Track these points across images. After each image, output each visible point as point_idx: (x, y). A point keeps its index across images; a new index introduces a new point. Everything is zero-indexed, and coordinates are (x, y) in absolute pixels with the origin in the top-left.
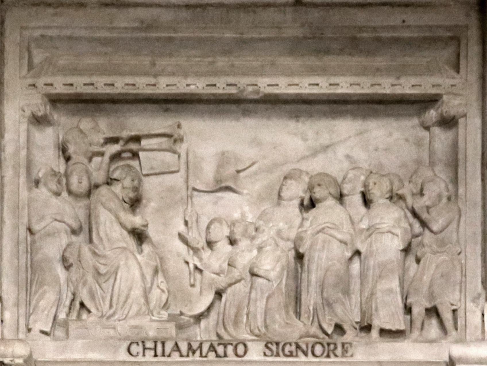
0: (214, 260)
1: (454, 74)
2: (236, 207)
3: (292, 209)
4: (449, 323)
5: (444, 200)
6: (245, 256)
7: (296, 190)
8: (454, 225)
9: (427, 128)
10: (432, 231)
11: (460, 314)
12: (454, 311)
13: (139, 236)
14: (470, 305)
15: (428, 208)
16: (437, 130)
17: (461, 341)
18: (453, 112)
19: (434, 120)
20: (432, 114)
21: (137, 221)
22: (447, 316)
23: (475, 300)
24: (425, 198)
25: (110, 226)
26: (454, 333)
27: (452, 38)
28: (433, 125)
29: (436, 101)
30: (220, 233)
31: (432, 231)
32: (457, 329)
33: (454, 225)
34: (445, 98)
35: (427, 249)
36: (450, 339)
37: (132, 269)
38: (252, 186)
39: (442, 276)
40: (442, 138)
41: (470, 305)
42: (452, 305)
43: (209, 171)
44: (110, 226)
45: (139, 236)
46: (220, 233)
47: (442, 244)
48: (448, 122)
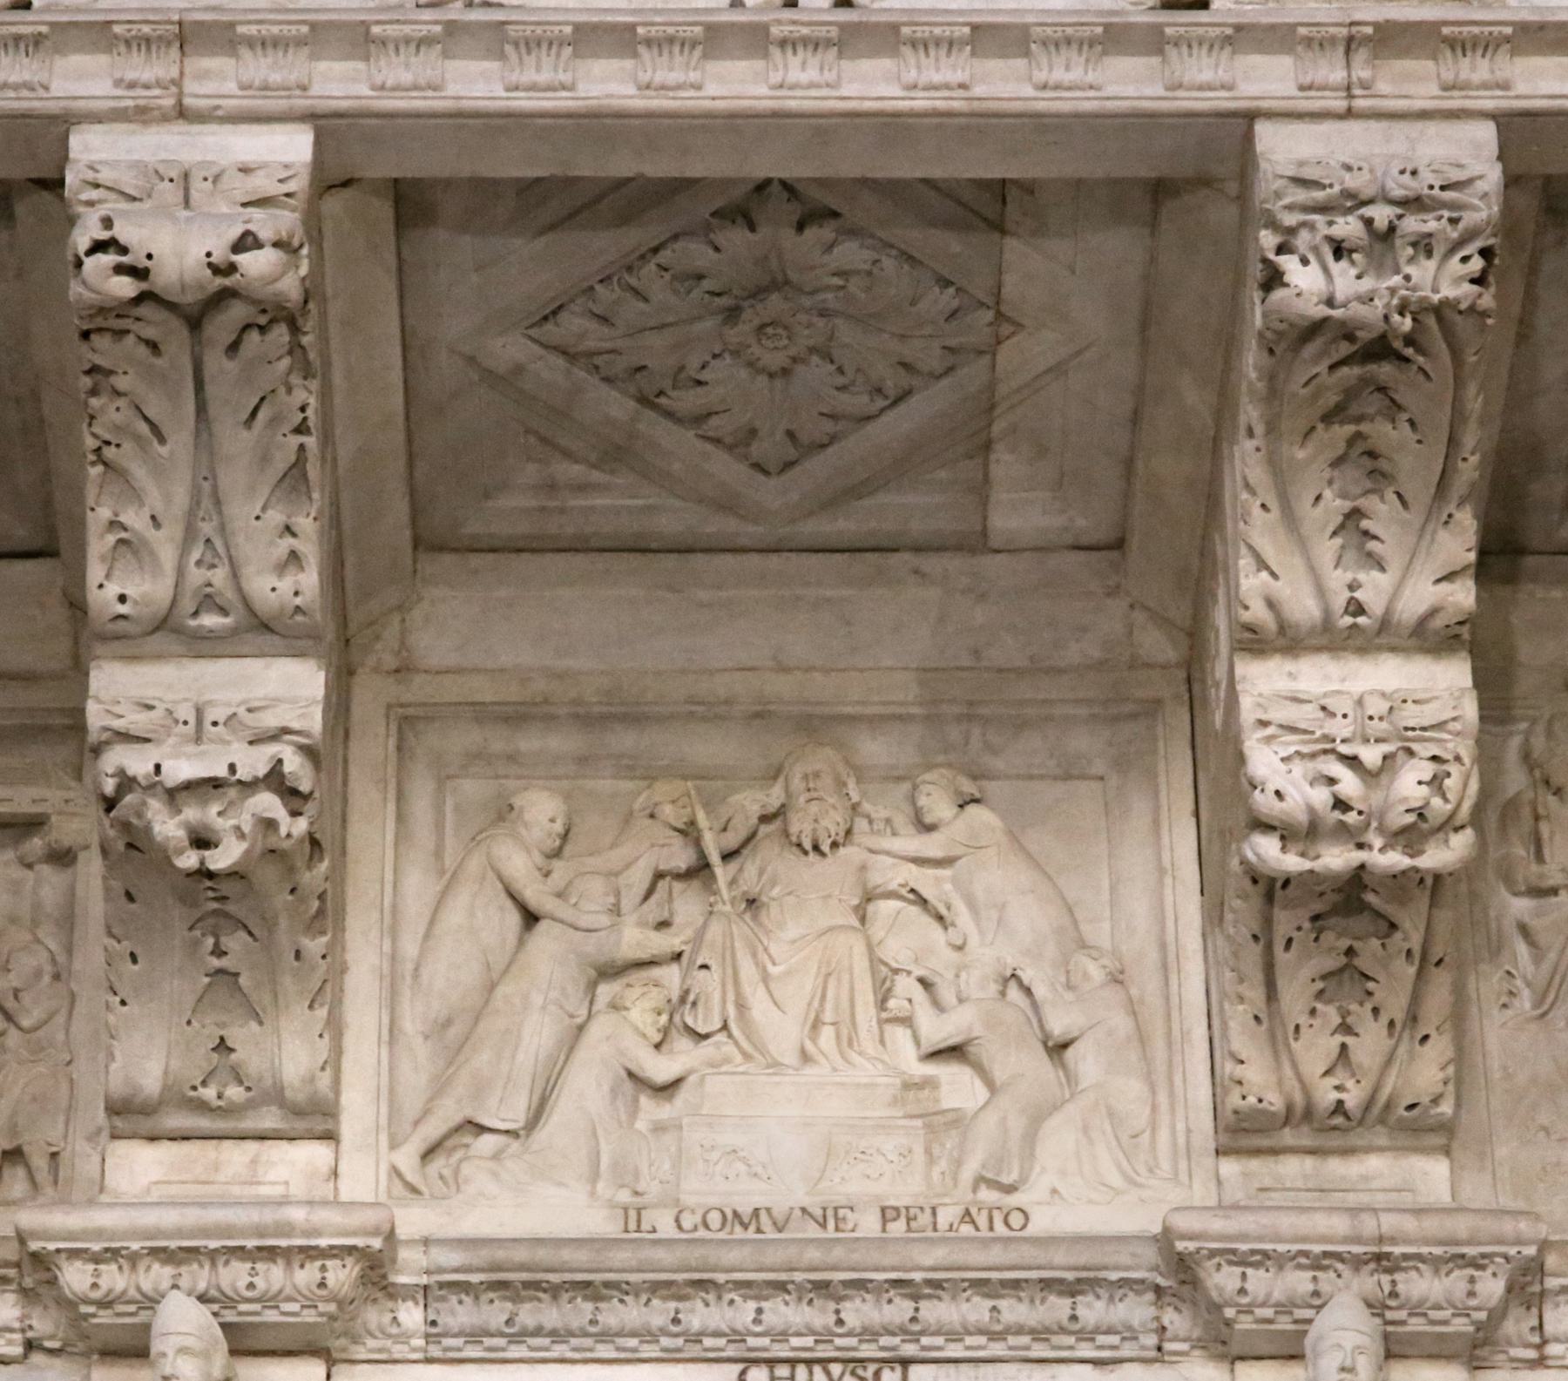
1: (73, 784)
4: (43, 1175)
5: (47, 979)
8: (60, 1019)
9: (30, 866)
10: (20, 1029)
11: (65, 1157)
12: (54, 1155)
14: (81, 1146)
15: (16, 993)
16: (45, 870)
17: (64, 1202)
18: (67, 842)
19: (40, 853)
20: (36, 844)
22: (40, 1162)
23: (92, 1137)
24: (11, 976)
26: (49, 1191)
27: (70, 728)
28: (40, 861)
29: (41, 824)
31: (20, 1029)
32: (56, 1182)
33: (60, 1019)
34: (53, 819)
35: (8, 1056)
36: (41, 1200)
39: (34, 1099)
40: (50, 884)
41: (81, 1146)
42: (50, 1145)
47: (37, 1050)
48: (63, 858)
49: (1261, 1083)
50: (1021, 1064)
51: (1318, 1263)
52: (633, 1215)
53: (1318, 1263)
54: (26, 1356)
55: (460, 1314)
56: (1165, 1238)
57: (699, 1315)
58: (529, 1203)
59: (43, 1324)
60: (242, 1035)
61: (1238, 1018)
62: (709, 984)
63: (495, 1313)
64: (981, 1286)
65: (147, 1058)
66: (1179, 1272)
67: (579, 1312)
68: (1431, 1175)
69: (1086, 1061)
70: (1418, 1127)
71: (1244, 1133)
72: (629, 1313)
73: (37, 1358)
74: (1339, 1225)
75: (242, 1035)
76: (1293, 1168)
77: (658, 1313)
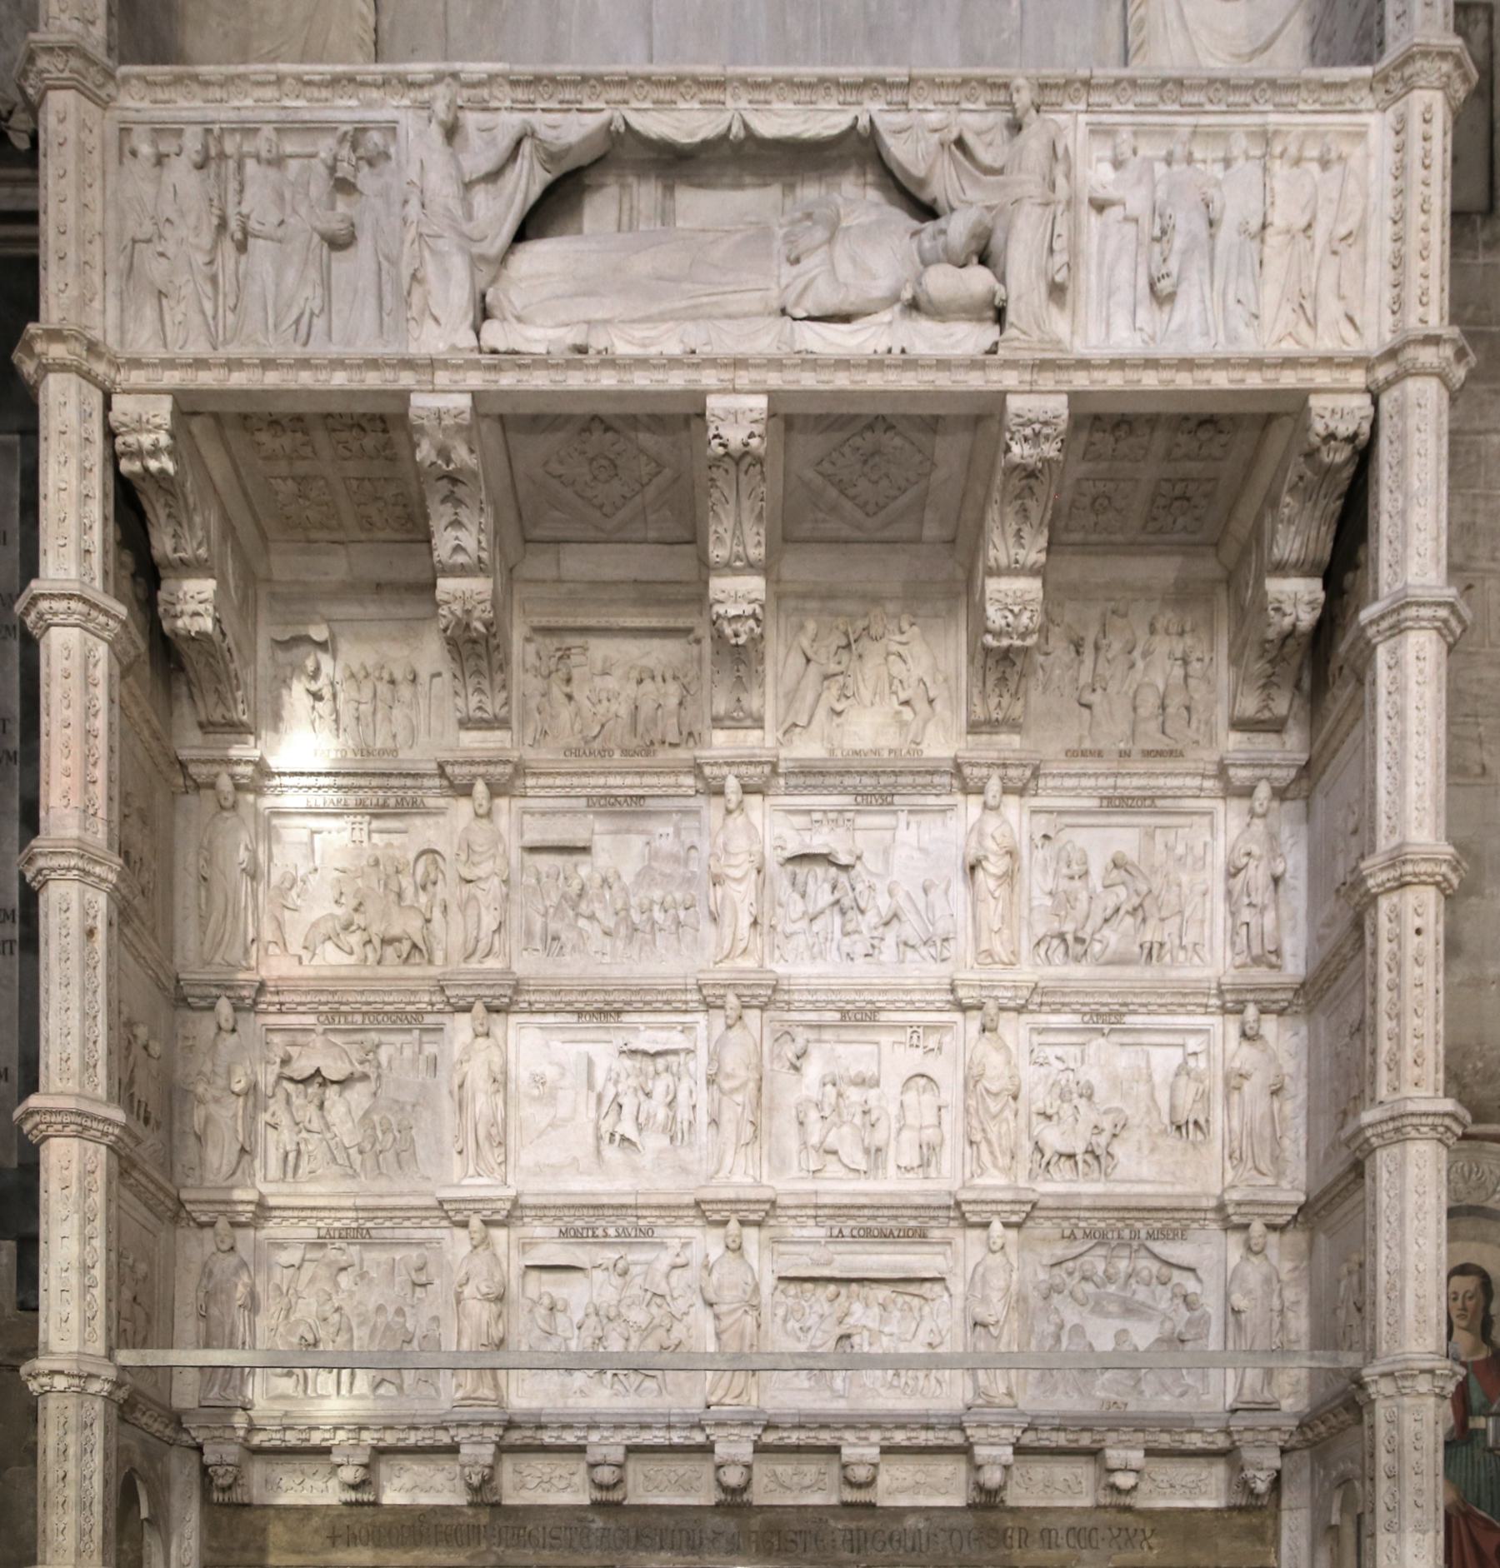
0: (601, 709)
2: (611, 683)
3: (634, 685)
6: (614, 707)
7: (635, 674)
13: (570, 697)
21: (568, 690)
25: (557, 692)
30: (604, 695)
37: (565, 713)
38: (618, 672)
43: (599, 666)
44: (557, 692)
45: (570, 697)
46: (604, 695)
49: (980, 713)
50: (921, 706)
51: (990, 766)
52: (832, 751)
53: (990, 766)
55: (793, 781)
56: (955, 758)
57: (848, 781)
58: (808, 748)
59: (700, 785)
60: (743, 696)
61: (976, 691)
62: (850, 681)
63: (801, 780)
64: (912, 773)
65: (721, 706)
66: (957, 769)
67: (818, 780)
68: (1015, 740)
69: (938, 705)
70: (1014, 726)
71: (974, 728)
72: (830, 781)
74: (994, 754)
75: (743, 696)
76: (984, 738)
77: (836, 781)
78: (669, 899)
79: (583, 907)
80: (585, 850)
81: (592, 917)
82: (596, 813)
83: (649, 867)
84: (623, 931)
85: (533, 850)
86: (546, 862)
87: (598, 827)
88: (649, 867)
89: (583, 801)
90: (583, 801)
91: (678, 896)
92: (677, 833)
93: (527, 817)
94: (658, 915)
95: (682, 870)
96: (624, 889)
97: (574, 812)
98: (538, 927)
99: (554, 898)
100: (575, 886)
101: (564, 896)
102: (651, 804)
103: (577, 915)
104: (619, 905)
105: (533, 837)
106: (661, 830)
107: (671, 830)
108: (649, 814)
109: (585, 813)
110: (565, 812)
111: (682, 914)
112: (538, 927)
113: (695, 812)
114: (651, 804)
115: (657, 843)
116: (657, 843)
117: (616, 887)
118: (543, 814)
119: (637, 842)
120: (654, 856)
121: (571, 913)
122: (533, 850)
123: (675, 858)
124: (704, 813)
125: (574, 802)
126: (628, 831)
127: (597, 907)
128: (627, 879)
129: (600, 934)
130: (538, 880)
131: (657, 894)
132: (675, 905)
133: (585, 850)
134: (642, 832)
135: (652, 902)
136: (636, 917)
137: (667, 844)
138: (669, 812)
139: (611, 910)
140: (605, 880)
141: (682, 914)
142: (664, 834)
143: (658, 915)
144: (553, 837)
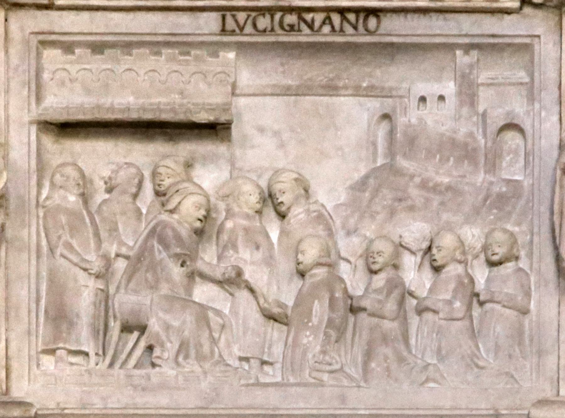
54: (521, 8)
73: (527, 10)
78: (447, 241)
79: (208, 257)
80: (215, 129)
81: (233, 281)
82: (241, 47)
83: (391, 169)
84: (319, 310)
85: (68, 128)
86: (101, 157)
87: (246, 77)
88: (391, 169)
89: (209, 23)
90: (209, 23)
91: (473, 235)
92: (468, 93)
93: (52, 56)
94: (415, 276)
95: (480, 178)
96: (321, 218)
97: (182, 45)
98: (84, 297)
99: (130, 238)
100: (190, 208)
101: (157, 233)
102: (395, 28)
103: (194, 276)
104: (311, 253)
105: (63, 101)
106: (422, 88)
107: (449, 88)
108: (392, 50)
109: (214, 48)
110: (156, 45)
111: (481, 275)
112: (84, 297)
113: (523, 49)
114: (395, 28)
115: (410, 117)
116: (410, 117)
117: (298, 214)
118: (98, 48)
119: (355, 115)
120: (400, 141)
121: (177, 272)
122: (68, 128)
123: (463, 152)
124: (546, 48)
125: (184, 23)
126: (331, 89)
127: (246, 258)
128: (330, 194)
129: (255, 317)
130: (85, 198)
131: (414, 231)
132: (463, 255)
133: (215, 129)
134: (371, 92)
135: (401, 246)
136: (354, 280)
137: (439, 120)
138: (450, 48)
139: (285, 266)
140: (269, 198)
141: (481, 275)
142: (431, 96)
143: (415, 276)
144: (125, 101)
